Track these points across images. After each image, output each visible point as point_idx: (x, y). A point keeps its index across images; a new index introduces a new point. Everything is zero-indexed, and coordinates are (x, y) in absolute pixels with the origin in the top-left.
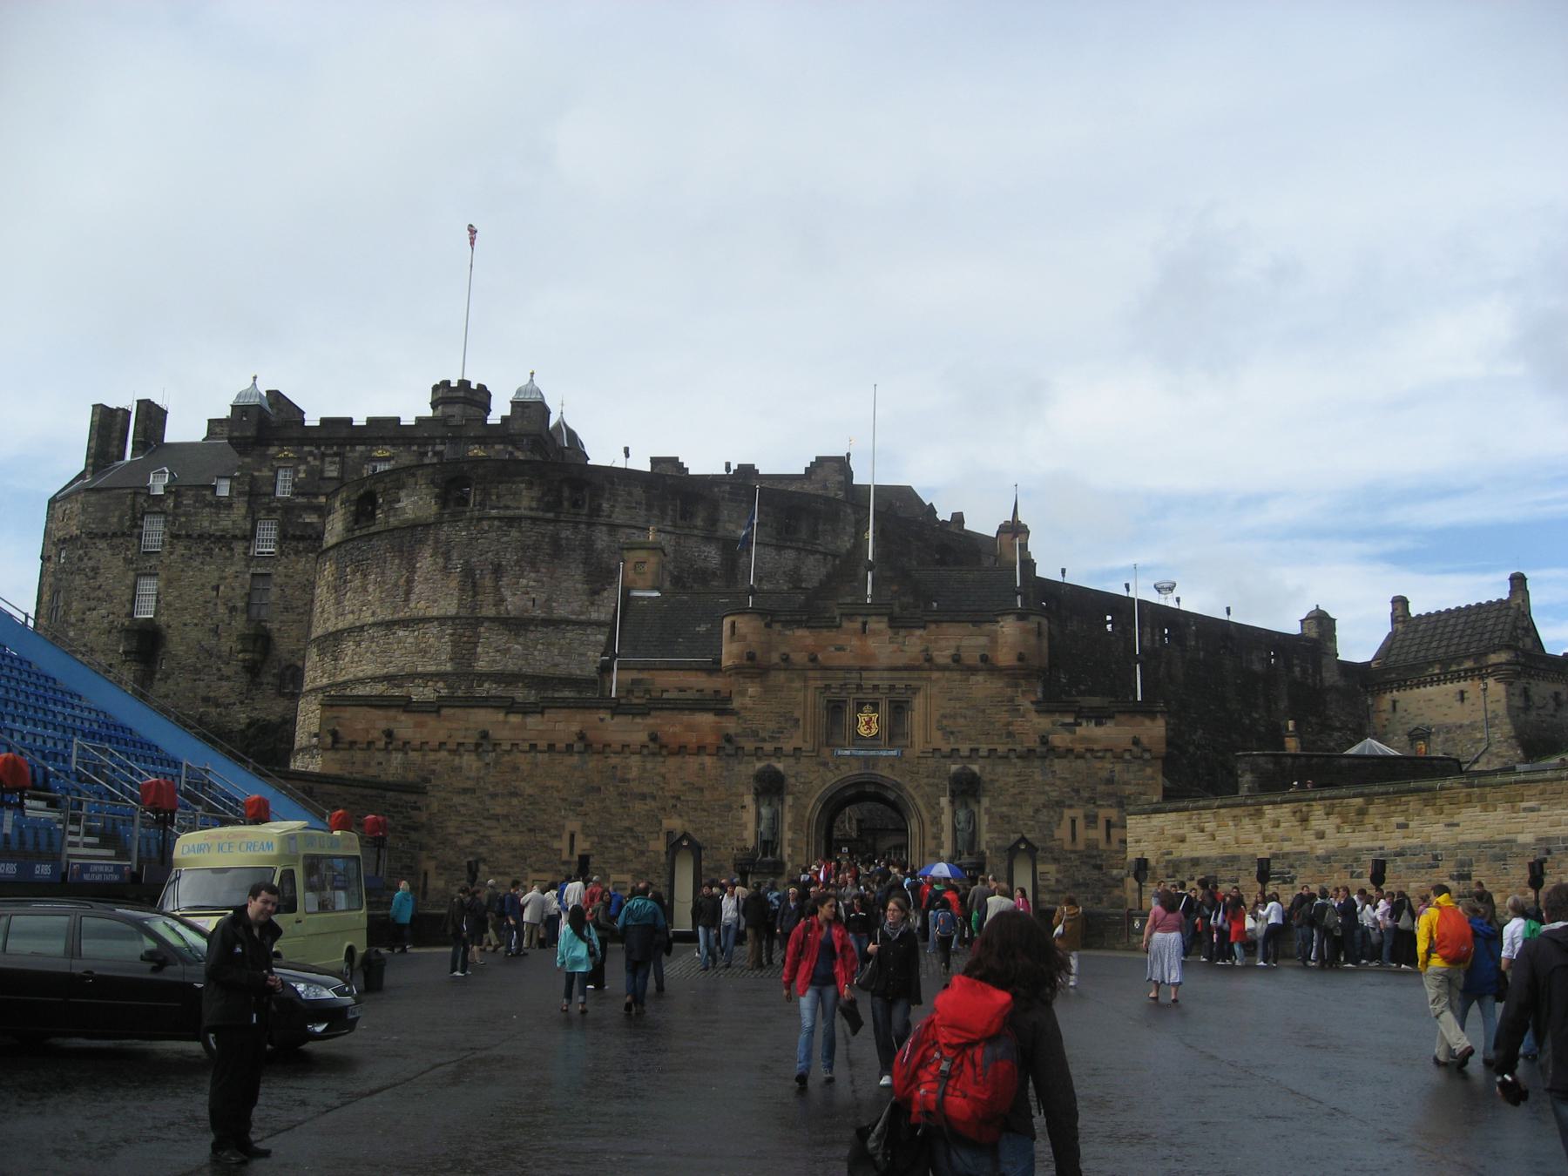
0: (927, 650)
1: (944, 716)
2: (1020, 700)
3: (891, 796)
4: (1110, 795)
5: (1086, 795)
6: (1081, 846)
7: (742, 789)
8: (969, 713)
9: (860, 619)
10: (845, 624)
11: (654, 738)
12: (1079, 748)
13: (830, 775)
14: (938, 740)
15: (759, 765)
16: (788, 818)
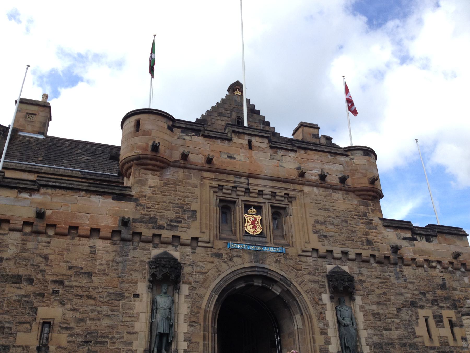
0: (299, 168)
1: (317, 222)
2: (371, 215)
3: (277, 291)
4: (447, 299)
5: (430, 297)
6: (437, 344)
7: (136, 276)
8: (336, 222)
9: (247, 138)
10: (236, 140)
11: (40, 215)
12: (420, 259)
13: (225, 266)
14: (315, 242)
15: (155, 252)
16: (184, 308)
